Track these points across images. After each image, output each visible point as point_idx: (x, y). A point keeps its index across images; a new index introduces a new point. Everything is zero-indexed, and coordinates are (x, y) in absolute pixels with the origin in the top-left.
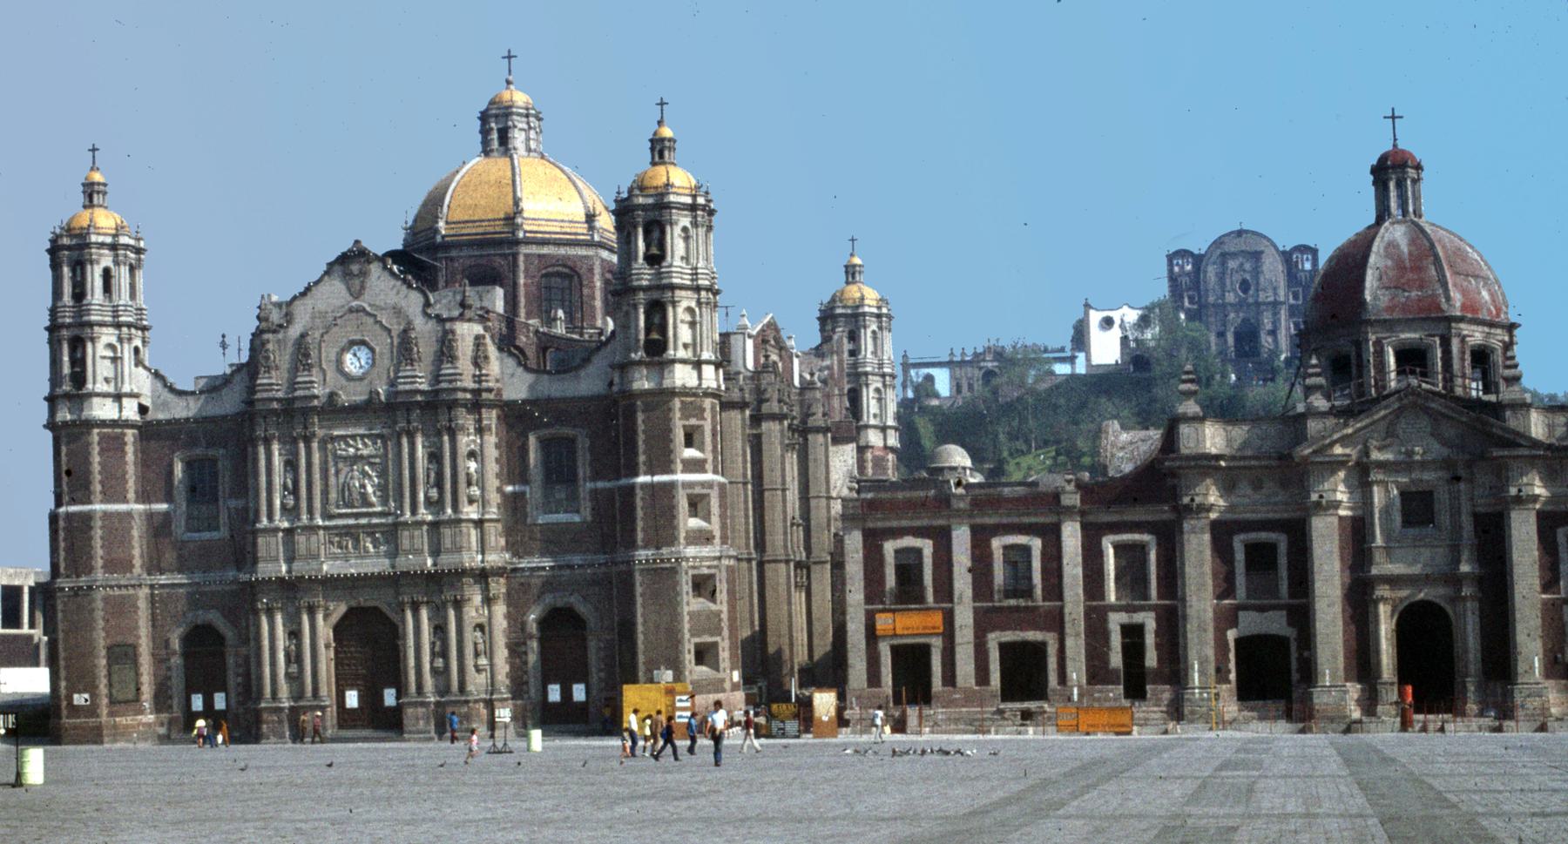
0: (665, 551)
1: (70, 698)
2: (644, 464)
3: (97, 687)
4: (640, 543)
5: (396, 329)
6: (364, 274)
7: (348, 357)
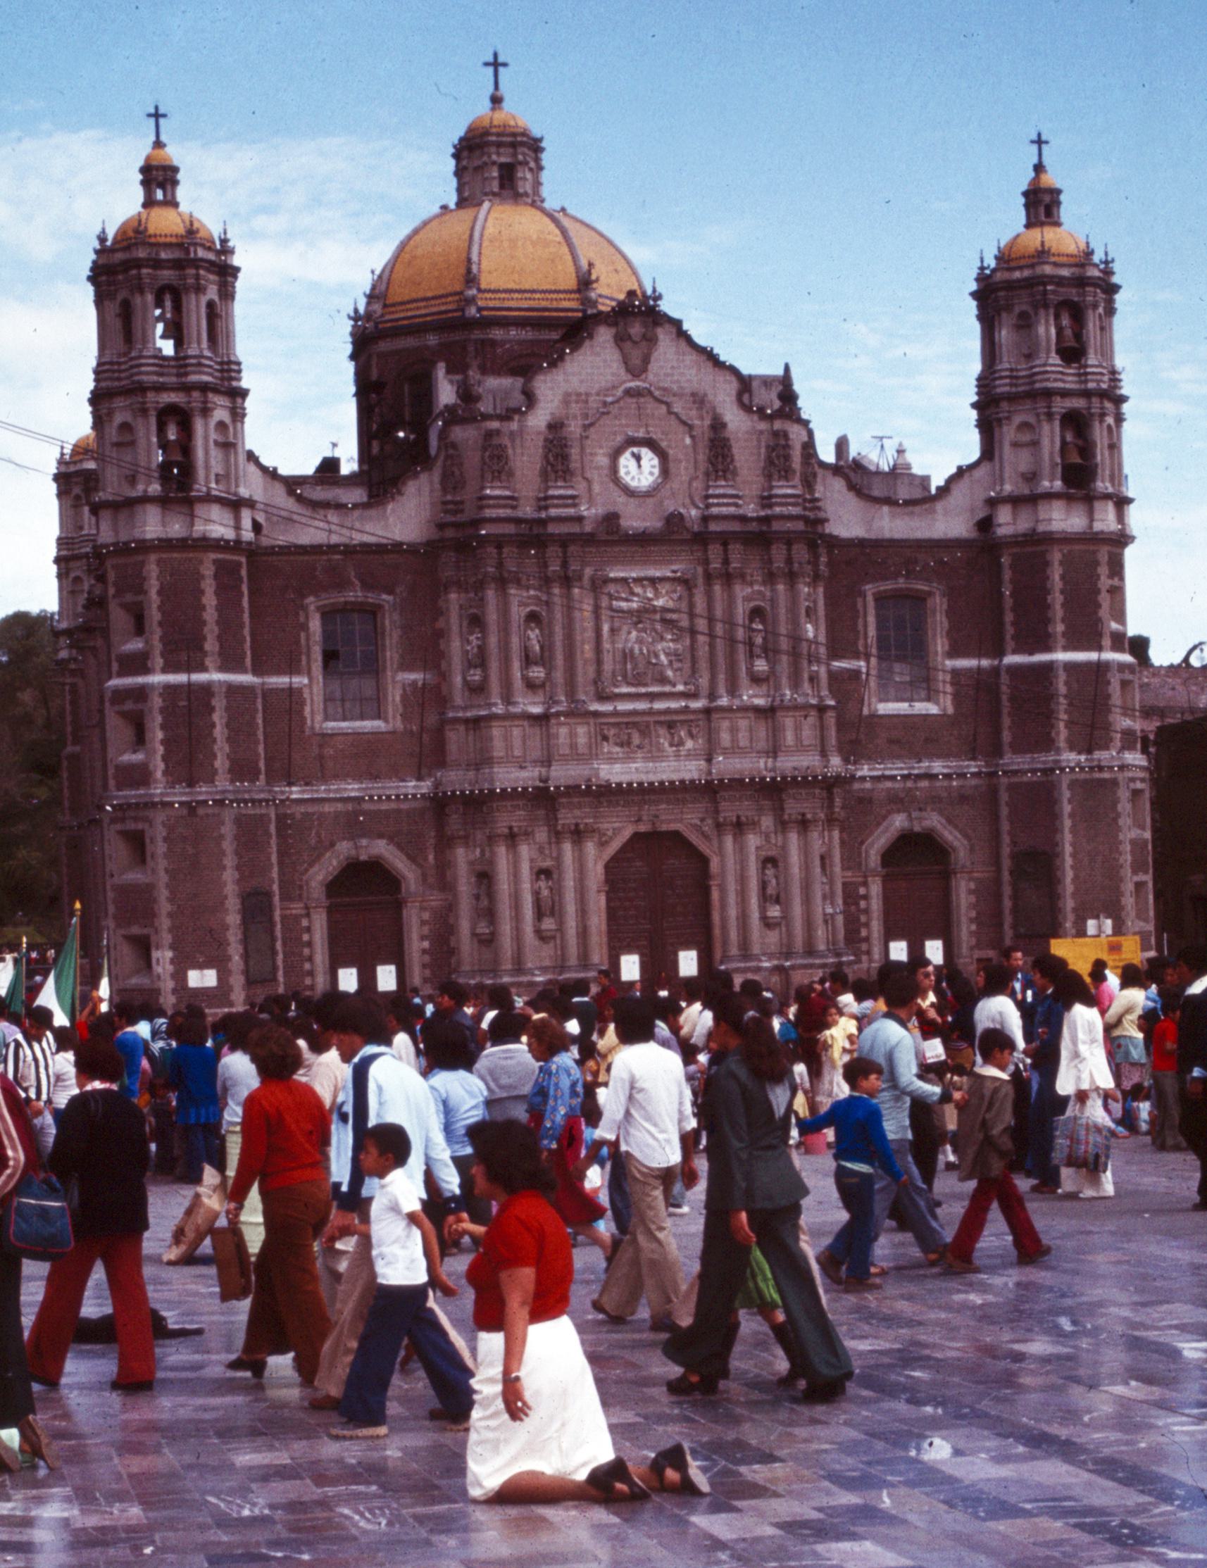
0: (1101, 756)
1: (180, 977)
2: (1064, 634)
3: (229, 959)
4: (1062, 744)
5: (702, 424)
6: (651, 341)
7: (626, 463)
